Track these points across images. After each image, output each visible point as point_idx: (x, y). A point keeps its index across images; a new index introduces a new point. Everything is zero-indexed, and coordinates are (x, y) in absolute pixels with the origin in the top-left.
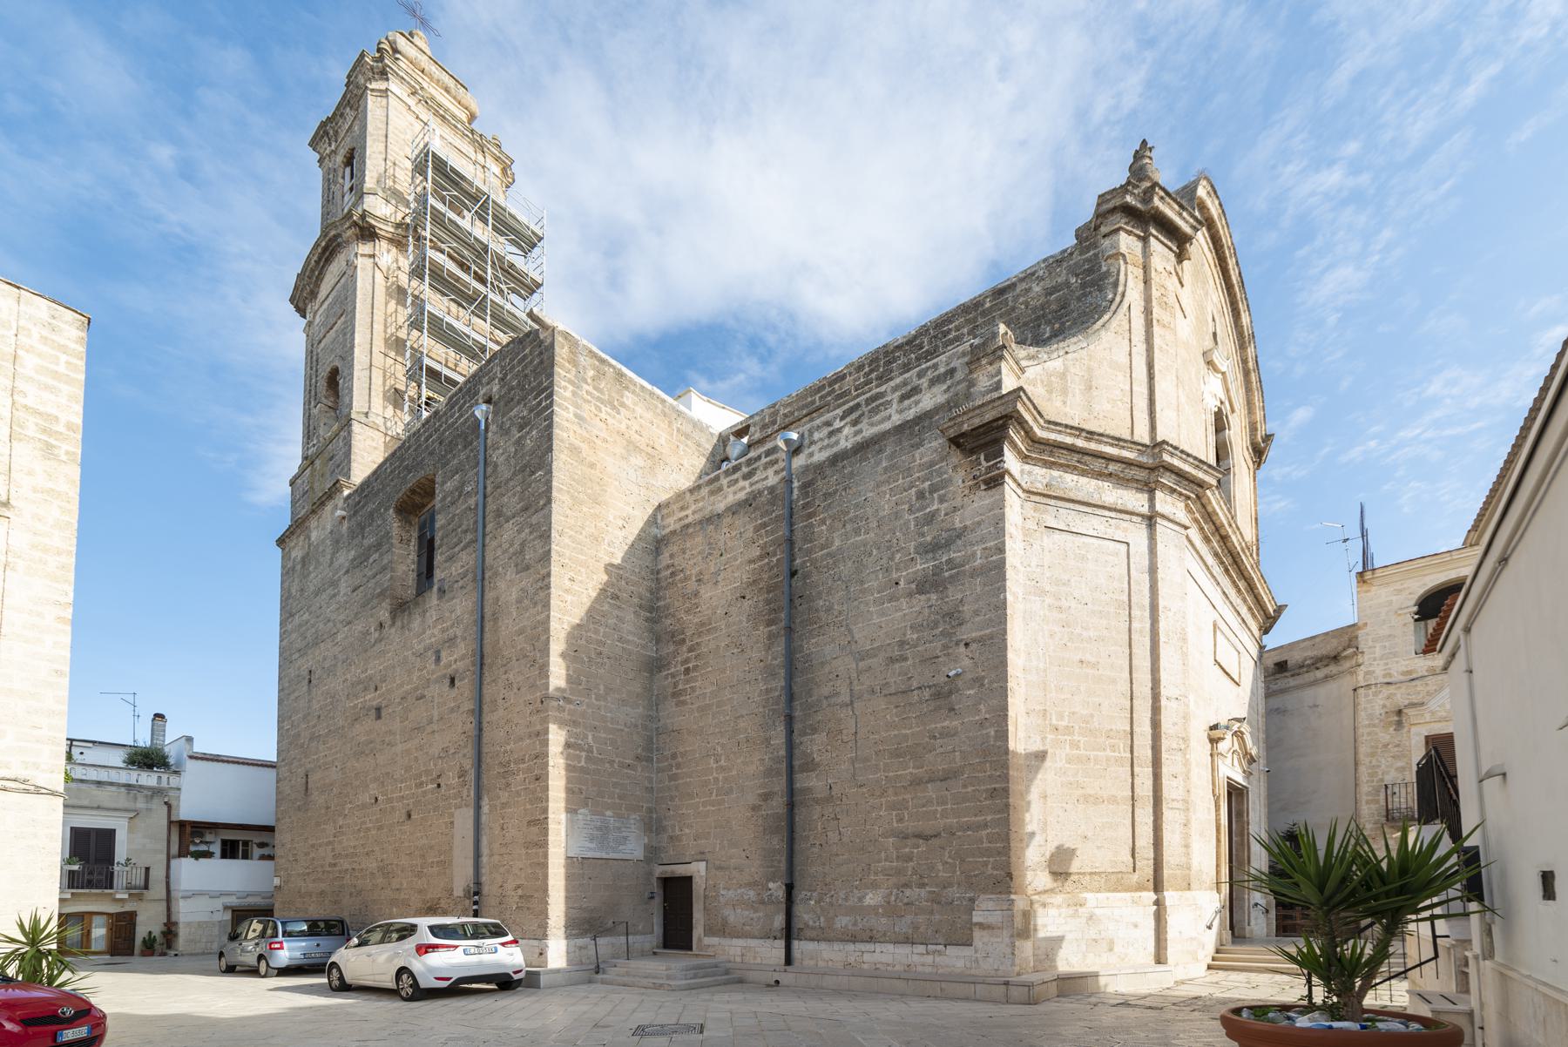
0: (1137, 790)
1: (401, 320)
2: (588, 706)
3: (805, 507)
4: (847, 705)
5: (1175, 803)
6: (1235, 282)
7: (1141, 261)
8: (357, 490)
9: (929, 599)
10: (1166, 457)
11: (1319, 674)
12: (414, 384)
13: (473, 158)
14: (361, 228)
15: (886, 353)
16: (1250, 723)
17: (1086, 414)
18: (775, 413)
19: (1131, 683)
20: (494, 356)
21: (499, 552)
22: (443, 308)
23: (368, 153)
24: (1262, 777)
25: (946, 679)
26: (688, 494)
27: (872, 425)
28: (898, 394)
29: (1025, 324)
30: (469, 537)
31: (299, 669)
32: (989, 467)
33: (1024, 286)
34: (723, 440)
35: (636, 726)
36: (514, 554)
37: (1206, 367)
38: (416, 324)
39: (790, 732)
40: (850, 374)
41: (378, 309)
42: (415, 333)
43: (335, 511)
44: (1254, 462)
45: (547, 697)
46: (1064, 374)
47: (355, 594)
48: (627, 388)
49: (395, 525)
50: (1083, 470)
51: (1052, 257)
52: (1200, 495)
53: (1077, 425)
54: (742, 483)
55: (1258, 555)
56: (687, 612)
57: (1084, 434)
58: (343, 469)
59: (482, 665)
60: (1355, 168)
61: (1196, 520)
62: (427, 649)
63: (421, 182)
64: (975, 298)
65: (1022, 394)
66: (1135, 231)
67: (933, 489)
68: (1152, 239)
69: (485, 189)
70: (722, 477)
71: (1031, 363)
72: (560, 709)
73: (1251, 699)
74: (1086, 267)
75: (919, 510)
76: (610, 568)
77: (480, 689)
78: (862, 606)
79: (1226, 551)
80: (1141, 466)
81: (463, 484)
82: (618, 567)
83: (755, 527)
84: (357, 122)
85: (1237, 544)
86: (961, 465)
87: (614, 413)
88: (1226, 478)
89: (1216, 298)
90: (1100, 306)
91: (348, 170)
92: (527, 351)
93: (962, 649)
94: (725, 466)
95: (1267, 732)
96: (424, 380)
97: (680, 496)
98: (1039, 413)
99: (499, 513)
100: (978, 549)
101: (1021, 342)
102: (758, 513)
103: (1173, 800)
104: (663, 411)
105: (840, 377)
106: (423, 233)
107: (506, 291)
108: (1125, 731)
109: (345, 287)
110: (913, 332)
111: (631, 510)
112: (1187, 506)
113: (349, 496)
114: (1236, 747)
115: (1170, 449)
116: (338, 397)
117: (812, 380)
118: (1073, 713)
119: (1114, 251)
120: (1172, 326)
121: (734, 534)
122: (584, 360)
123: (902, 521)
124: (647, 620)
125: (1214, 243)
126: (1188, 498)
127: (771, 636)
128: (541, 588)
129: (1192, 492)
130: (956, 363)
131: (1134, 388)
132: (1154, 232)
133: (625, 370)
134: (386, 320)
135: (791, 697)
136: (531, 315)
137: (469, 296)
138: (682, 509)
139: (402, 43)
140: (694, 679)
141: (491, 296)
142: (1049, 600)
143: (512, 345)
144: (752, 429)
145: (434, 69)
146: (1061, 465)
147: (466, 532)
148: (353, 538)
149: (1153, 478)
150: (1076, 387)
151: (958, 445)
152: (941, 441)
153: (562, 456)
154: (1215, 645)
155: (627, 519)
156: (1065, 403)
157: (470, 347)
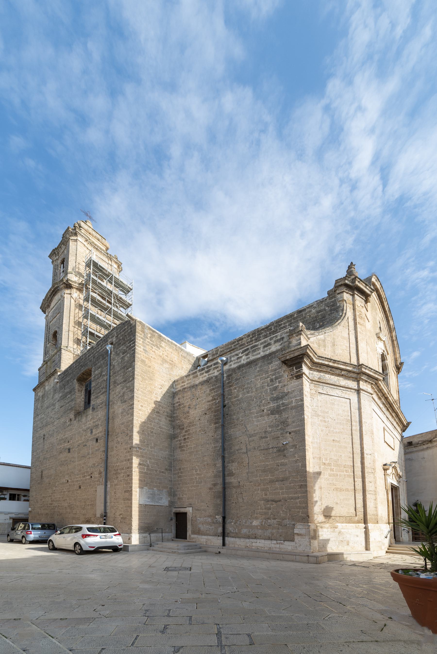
0: (356, 487)
1: (80, 315)
2: (147, 450)
3: (228, 383)
4: (245, 453)
5: (371, 492)
6: (387, 310)
7: (352, 302)
8: (63, 373)
9: (275, 417)
10: (363, 370)
11: (425, 447)
12: (85, 337)
13: (107, 262)
14: (66, 285)
15: (258, 331)
16: (399, 464)
17: (333, 354)
18: (218, 350)
19: (353, 448)
20: (114, 328)
21: (115, 396)
22: (95, 312)
23: (69, 260)
24: (404, 483)
25: (282, 445)
26: (185, 378)
27: (253, 356)
28: (263, 345)
29: (310, 323)
30: (104, 390)
31: (40, 434)
32: (297, 371)
33: (309, 310)
34: (198, 359)
35: (165, 458)
36: (120, 396)
37: (377, 339)
38: (86, 317)
39: (224, 462)
40: (245, 338)
41: (72, 312)
42: (85, 320)
43: (55, 380)
44: (396, 372)
45: (132, 447)
46: (324, 340)
47: (61, 408)
48: (162, 341)
49: (77, 385)
50: (332, 373)
51: (319, 300)
52: (377, 383)
53: (330, 358)
54: (205, 374)
55: (399, 404)
56: (185, 418)
57: (332, 361)
58: (58, 365)
59: (108, 435)
60: (433, 270)
61: (375, 392)
62: (88, 429)
63: (89, 270)
64: (291, 313)
65: (309, 347)
66: (349, 292)
67: (276, 378)
68: (356, 295)
69: (112, 273)
70: (198, 372)
71: (312, 336)
72: (137, 451)
73: (399, 455)
74: (332, 304)
75: (271, 385)
76: (156, 402)
77: (107, 443)
78: (250, 419)
79: (387, 403)
80: (354, 372)
81: (102, 372)
82: (159, 402)
83: (210, 390)
84: (66, 250)
85: (391, 400)
86: (286, 371)
87: (158, 349)
88: (386, 377)
89: (380, 315)
90: (337, 317)
91: (62, 265)
92: (126, 327)
93: (288, 434)
94: (199, 368)
95: (406, 467)
96: (88, 336)
97: (182, 378)
98: (315, 353)
99: (115, 382)
100: (294, 400)
101: (308, 329)
102: (211, 385)
103: (370, 491)
104: (176, 349)
105: (241, 339)
106: (89, 287)
107: (119, 306)
108: (351, 465)
109: (60, 304)
110: (268, 324)
111: (164, 382)
112: (372, 387)
113: (60, 375)
114: (394, 472)
115: (365, 367)
116: (57, 341)
117: (231, 339)
118: (331, 459)
119: (342, 299)
120: (364, 325)
121: (202, 392)
122: (146, 331)
123: (265, 389)
124: (170, 421)
125: (379, 297)
126: (372, 384)
127: (216, 428)
128: (130, 409)
129: (373, 382)
130: (284, 335)
131: (351, 346)
132: (356, 293)
133: (162, 334)
134: (75, 315)
135: (224, 450)
136: (127, 315)
137: (105, 308)
138: (183, 382)
139: (82, 224)
140: (188, 442)
141: (113, 308)
142: (320, 418)
143: (120, 325)
144: (209, 356)
145: (94, 233)
146: (324, 371)
147: (102, 388)
148: (61, 389)
149: (358, 376)
150: (329, 345)
151: (285, 364)
152: (279, 362)
153: (139, 363)
154: (384, 436)
155: (162, 386)
156: (325, 350)
157: (105, 325)
